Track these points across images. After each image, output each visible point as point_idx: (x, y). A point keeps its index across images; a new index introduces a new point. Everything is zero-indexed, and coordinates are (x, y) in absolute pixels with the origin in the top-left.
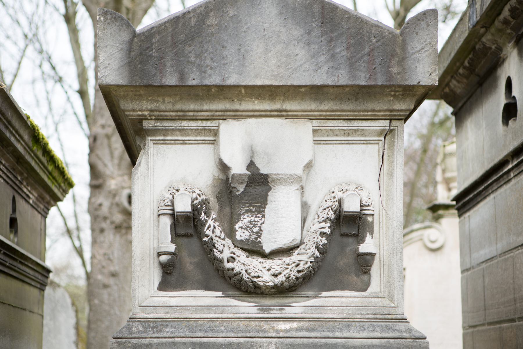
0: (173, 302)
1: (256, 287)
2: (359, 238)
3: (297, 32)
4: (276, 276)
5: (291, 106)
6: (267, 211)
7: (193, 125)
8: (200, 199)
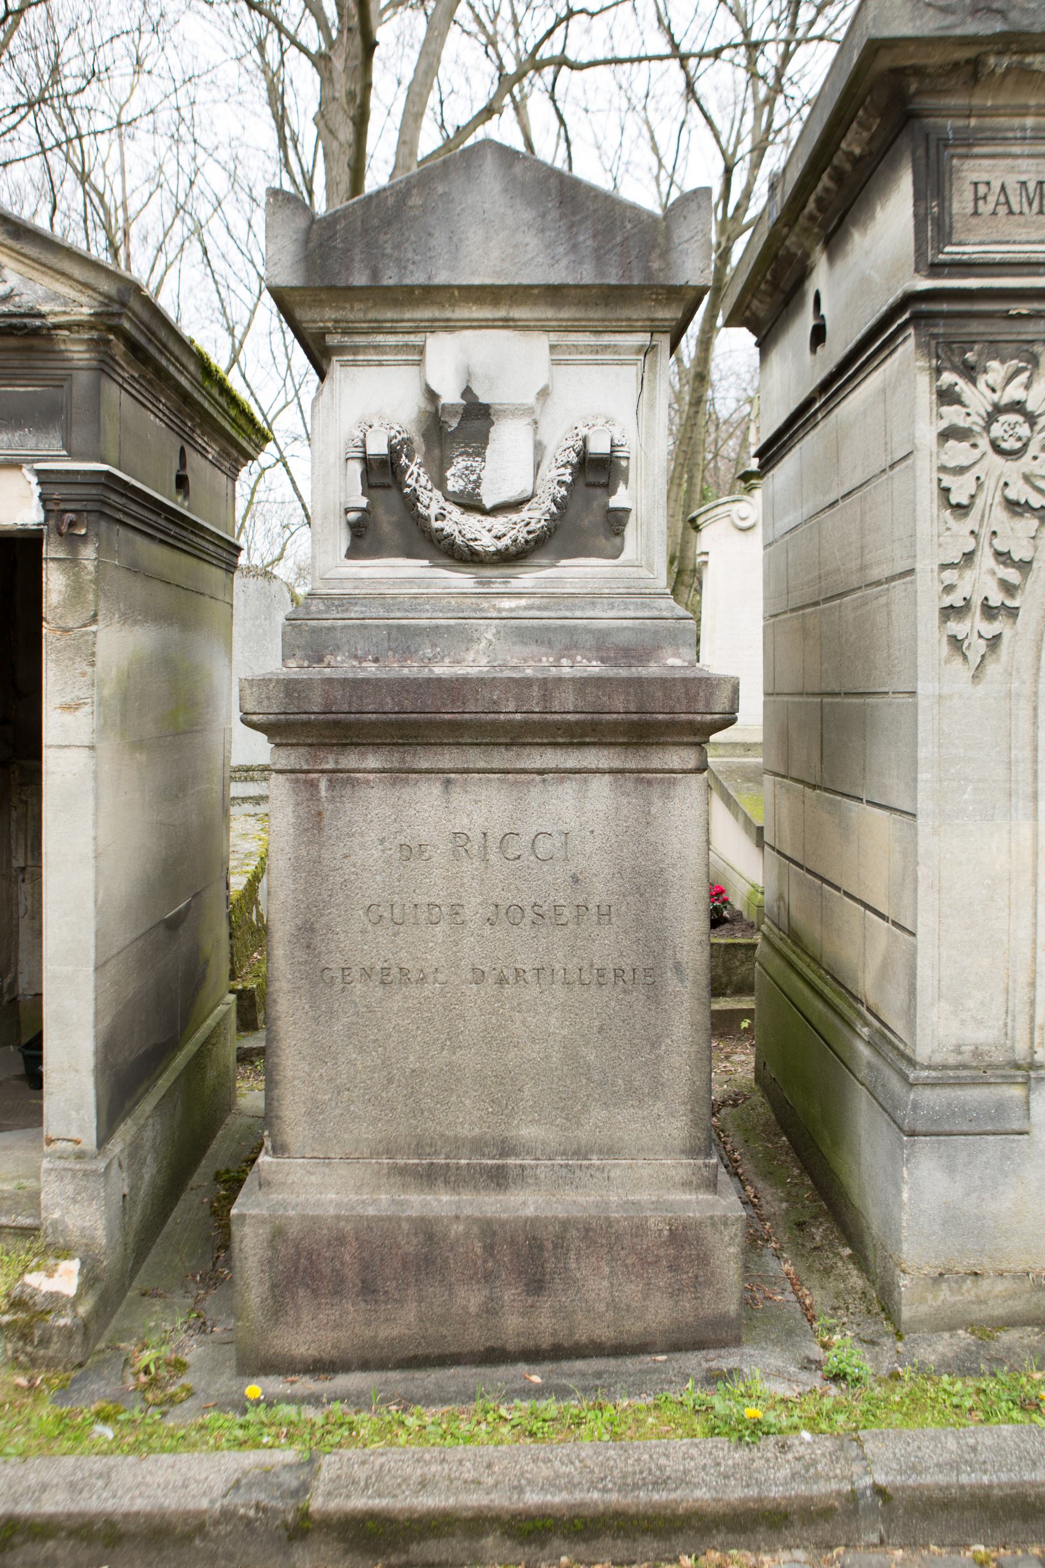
0: (365, 573)
1: (474, 553)
2: (610, 489)
3: (528, 215)
4: (498, 538)
5: (519, 313)
6: (488, 452)
7: (391, 340)
8: (399, 438)
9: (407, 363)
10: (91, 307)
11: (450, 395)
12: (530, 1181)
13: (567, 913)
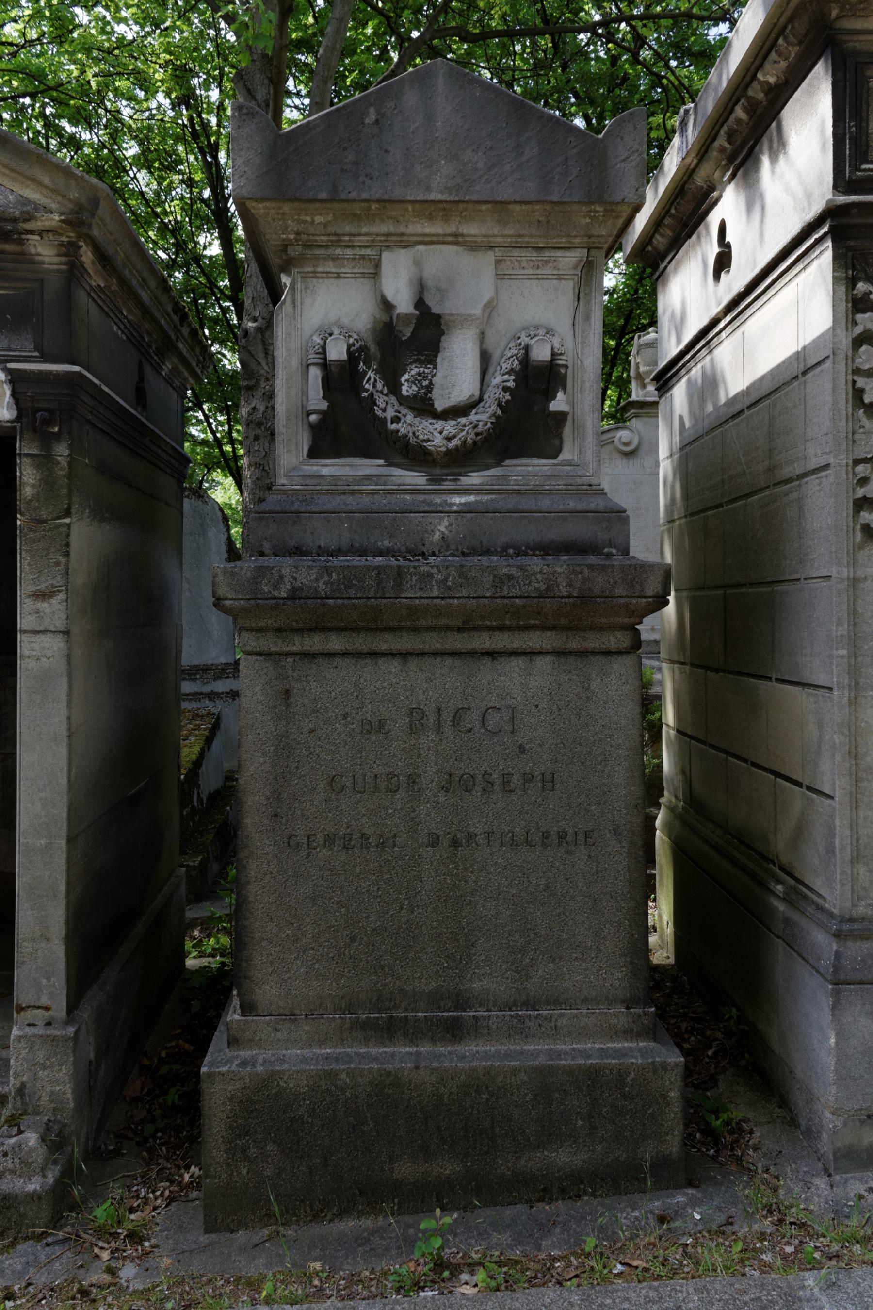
1: (426, 452)
4: (449, 439)
6: (439, 360)
8: (357, 345)
9: (363, 275)
10: (61, 214)
11: (404, 304)
12: (484, 1032)
13: (516, 780)
